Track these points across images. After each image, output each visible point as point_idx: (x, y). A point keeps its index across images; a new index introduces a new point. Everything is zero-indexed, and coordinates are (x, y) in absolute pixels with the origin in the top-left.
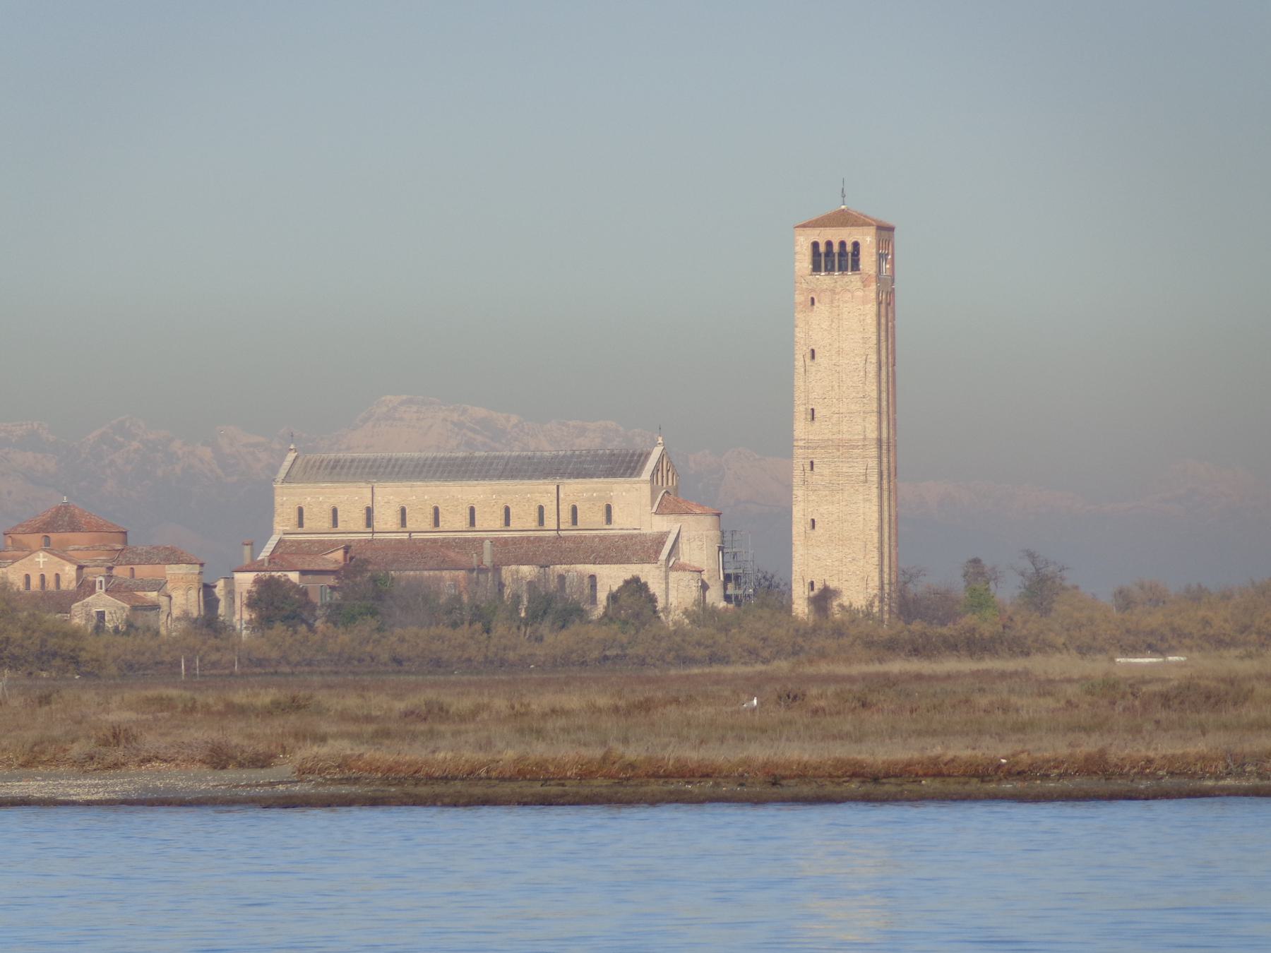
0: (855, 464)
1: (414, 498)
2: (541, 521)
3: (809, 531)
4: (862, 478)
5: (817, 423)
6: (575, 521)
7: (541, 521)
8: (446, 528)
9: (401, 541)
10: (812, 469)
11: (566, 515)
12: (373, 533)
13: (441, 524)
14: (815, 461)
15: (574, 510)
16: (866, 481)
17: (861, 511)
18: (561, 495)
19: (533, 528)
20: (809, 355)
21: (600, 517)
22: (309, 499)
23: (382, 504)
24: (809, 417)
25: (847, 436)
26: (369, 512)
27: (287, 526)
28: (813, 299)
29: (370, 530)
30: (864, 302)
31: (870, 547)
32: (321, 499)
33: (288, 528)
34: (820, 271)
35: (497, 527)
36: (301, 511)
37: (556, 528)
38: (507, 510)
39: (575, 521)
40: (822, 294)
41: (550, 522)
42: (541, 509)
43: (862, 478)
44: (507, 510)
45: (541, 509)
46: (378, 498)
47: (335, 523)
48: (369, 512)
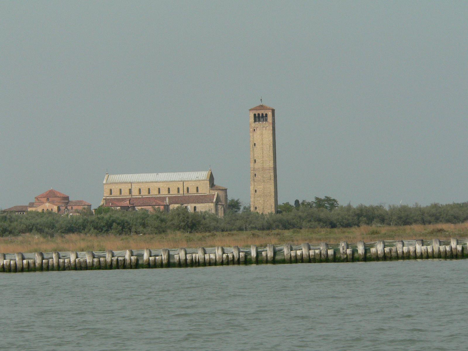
2: (178, 192)
6: (188, 191)
7: (178, 192)
10: (255, 176)
12: (132, 196)
15: (188, 189)
18: (184, 185)
20: (254, 145)
21: (195, 191)
26: (130, 190)
28: (254, 130)
29: (130, 195)
33: (108, 195)
36: (111, 190)
39: (188, 191)
46: (133, 187)
48: (130, 190)
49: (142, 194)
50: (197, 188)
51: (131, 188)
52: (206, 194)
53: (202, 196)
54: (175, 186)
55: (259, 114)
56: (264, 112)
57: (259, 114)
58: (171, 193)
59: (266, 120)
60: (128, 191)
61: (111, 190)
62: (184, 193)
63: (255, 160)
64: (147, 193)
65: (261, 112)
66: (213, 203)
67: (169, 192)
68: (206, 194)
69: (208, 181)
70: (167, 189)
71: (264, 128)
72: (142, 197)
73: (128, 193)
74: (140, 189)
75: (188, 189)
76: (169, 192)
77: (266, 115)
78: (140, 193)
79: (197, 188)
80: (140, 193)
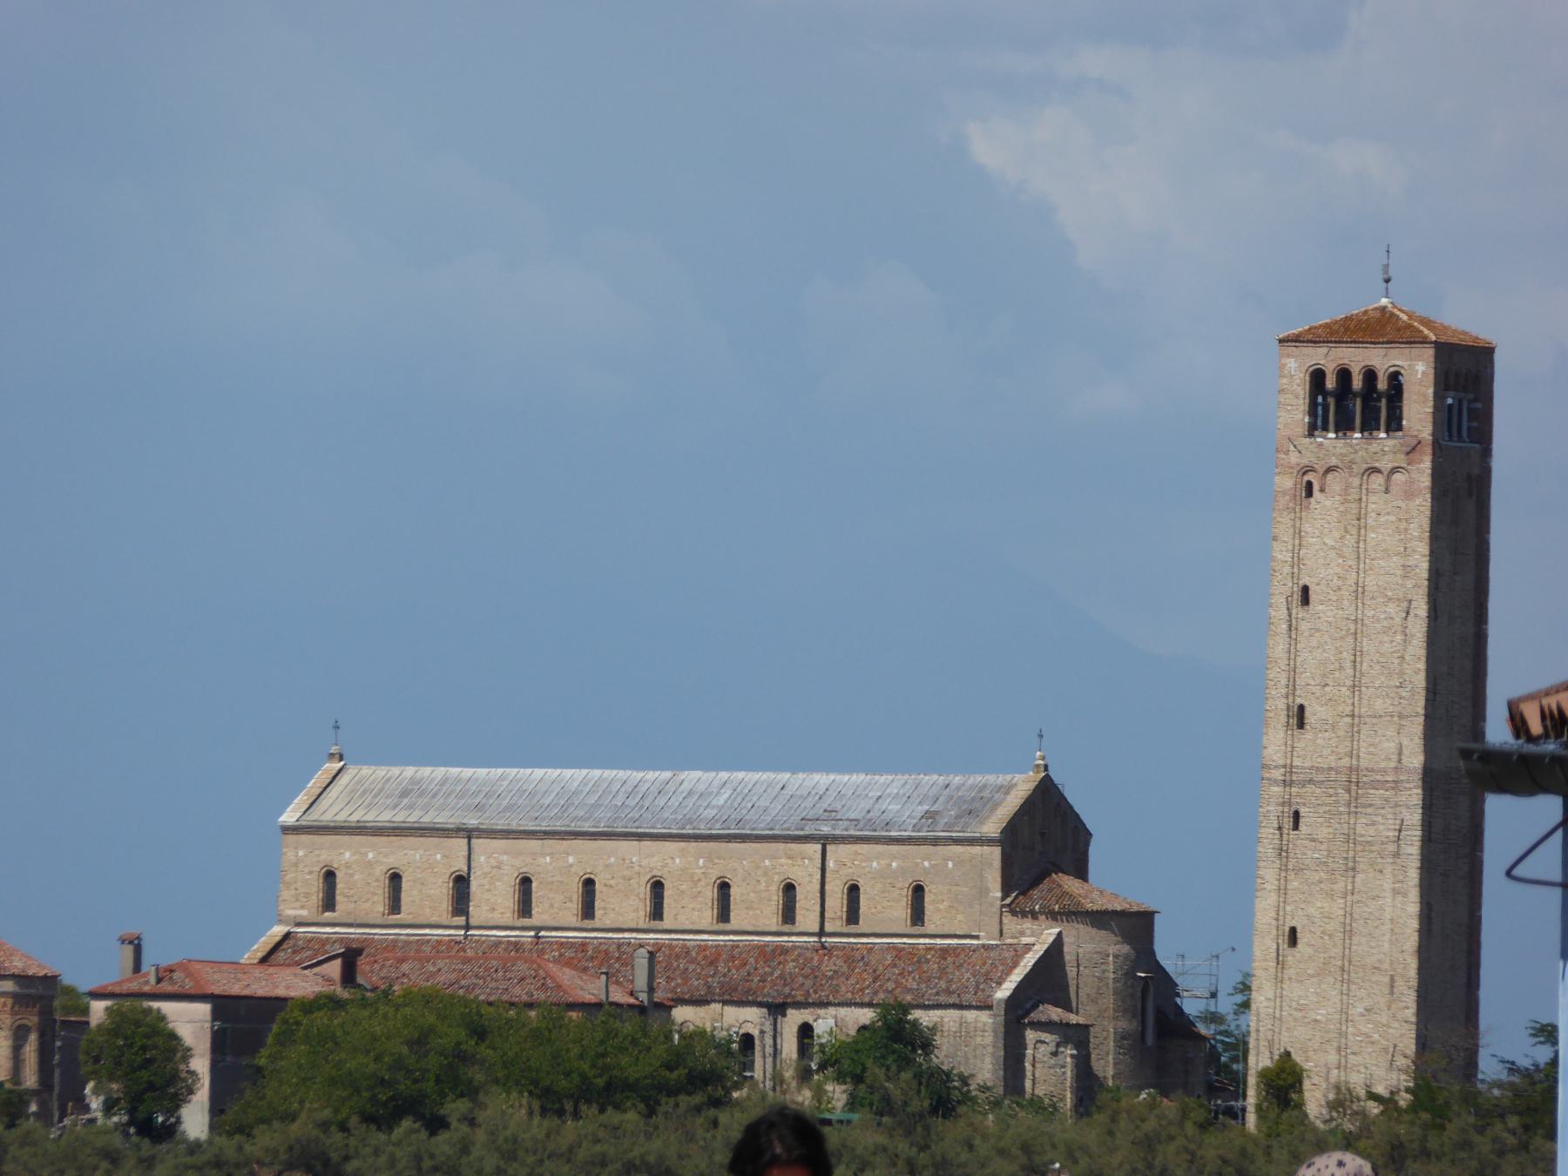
0: (1379, 819)
1: (548, 859)
2: (789, 914)
3: (1284, 946)
4: (1392, 848)
5: (1308, 735)
6: (853, 915)
7: (789, 914)
8: (608, 923)
9: (517, 946)
10: (1296, 827)
11: (837, 902)
12: (467, 927)
13: (598, 913)
14: (1303, 811)
15: (854, 890)
16: (1397, 855)
17: (1387, 916)
18: (831, 864)
19: (774, 929)
20: (1297, 597)
21: (899, 912)
22: (347, 854)
23: (487, 870)
24: (1294, 721)
25: (1364, 763)
26: (461, 883)
27: (302, 907)
28: (1309, 485)
29: (461, 920)
30: (1409, 495)
31: (1399, 982)
32: (371, 855)
33: (304, 913)
34: (1352, 429)
35: (705, 924)
36: (330, 876)
37: (816, 929)
38: (724, 887)
39: (853, 915)
40: (1330, 476)
41: (807, 917)
42: (789, 889)
43: (1392, 848)
44: (724, 887)
45: (789, 889)
46: (480, 860)
47: (395, 905)
48: (461, 883)
49: (539, 915)
50: (918, 891)
51: (466, 869)
52: (975, 942)
53: (945, 952)
54: (765, 874)
55: (1344, 375)
56: (1382, 359)
57: (1344, 375)
58: (738, 919)
59: (1395, 423)
60: (442, 891)
61: (330, 876)
62: (828, 928)
63: (1301, 708)
64: (569, 912)
65: (1357, 358)
66: (990, 1007)
67: (724, 914)
68: (977, 937)
69: (989, 842)
70: (711, 894)
71: (1377, 481)
72: (537, 937)
73: (445, 905)
74: (526, 882)
75: (854, 890)
76: (724, 914)
77: (1395, 377)
78: (525, 907)
79: (918, 891)
80: (525, 907)
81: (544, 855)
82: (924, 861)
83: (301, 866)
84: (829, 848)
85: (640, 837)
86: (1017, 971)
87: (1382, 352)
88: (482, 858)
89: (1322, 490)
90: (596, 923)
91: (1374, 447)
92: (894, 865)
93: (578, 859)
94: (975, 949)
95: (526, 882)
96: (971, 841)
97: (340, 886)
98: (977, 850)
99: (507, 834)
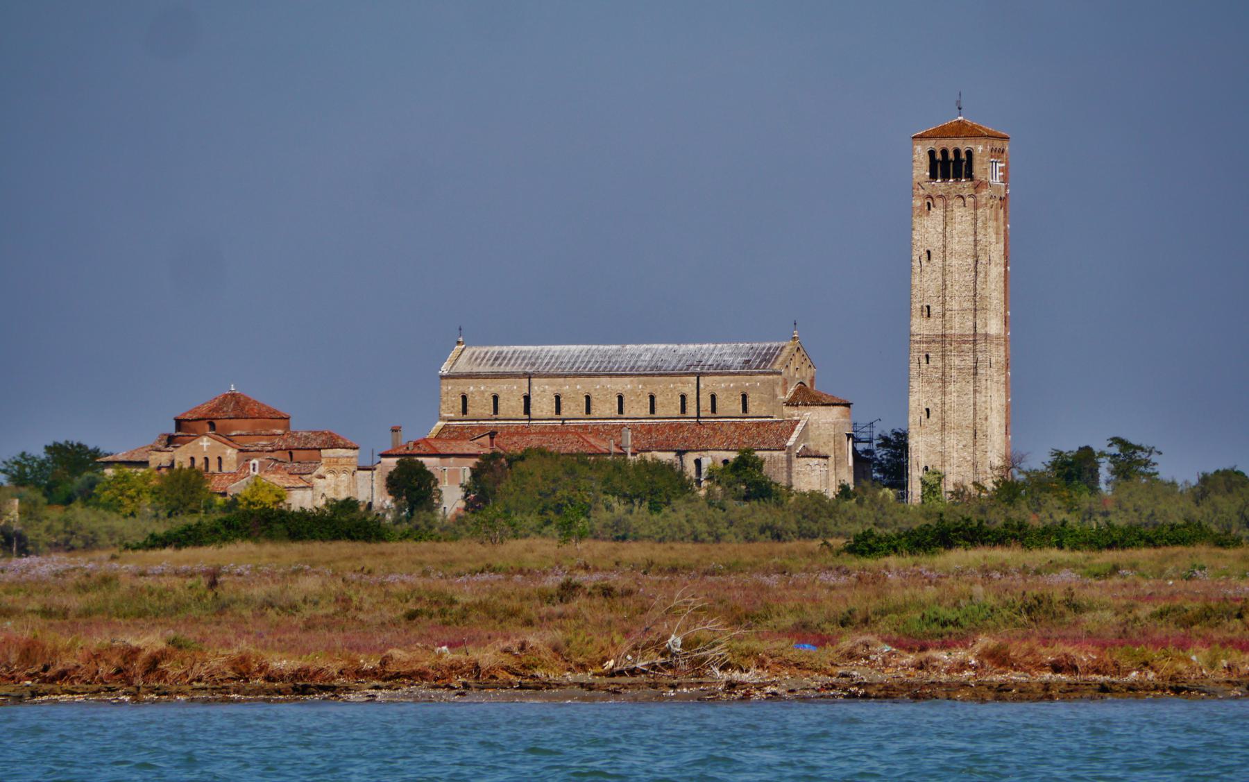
0: (967, 358)
2: (683, 409)
6: (714, 410)
7: (683, 409)
8: (597, 416)
9: (554, 427)
11: (706, 402)
12: (530, 419)
15: (713, 397)
18: (702, 386)
22: (472, 388)
23: (539, 392)
24: (925, 314)
26: (527, 399)
27: (451, 413)
32: (482, 388)
33: (452, 415)
37: (696, 415)
38: (652, 398)
39: (714, 410)
41: (691, 410)
42: (683, 397)
44: (652, 398)
45: (683, 397)
46: (535, 388)
48: (527, 399)
50: (744, 397)
53: (758, 425)
56: (963, 145)
58: (659, 412)
65: (951, 144)
68: (772, 417)
72: (563, 423)
75: (713, 397)
80: (558, 411)
81: (565, 385)
82: (746, 382)
83: (450, 394)
84: (701, 378)
85: (610, 376)
86: (795, 432)
87: (962, 141)
88: (536, 388)
89: (934, 206)
90: (592, 416)
91: (959, 186)
92: (732, 385)
93: (581, 386)
94: (771, 423)
95: (558, 398)
96: (769, 374)
97: (469, 402)
98: (771, 377)
99: (548, 376)
